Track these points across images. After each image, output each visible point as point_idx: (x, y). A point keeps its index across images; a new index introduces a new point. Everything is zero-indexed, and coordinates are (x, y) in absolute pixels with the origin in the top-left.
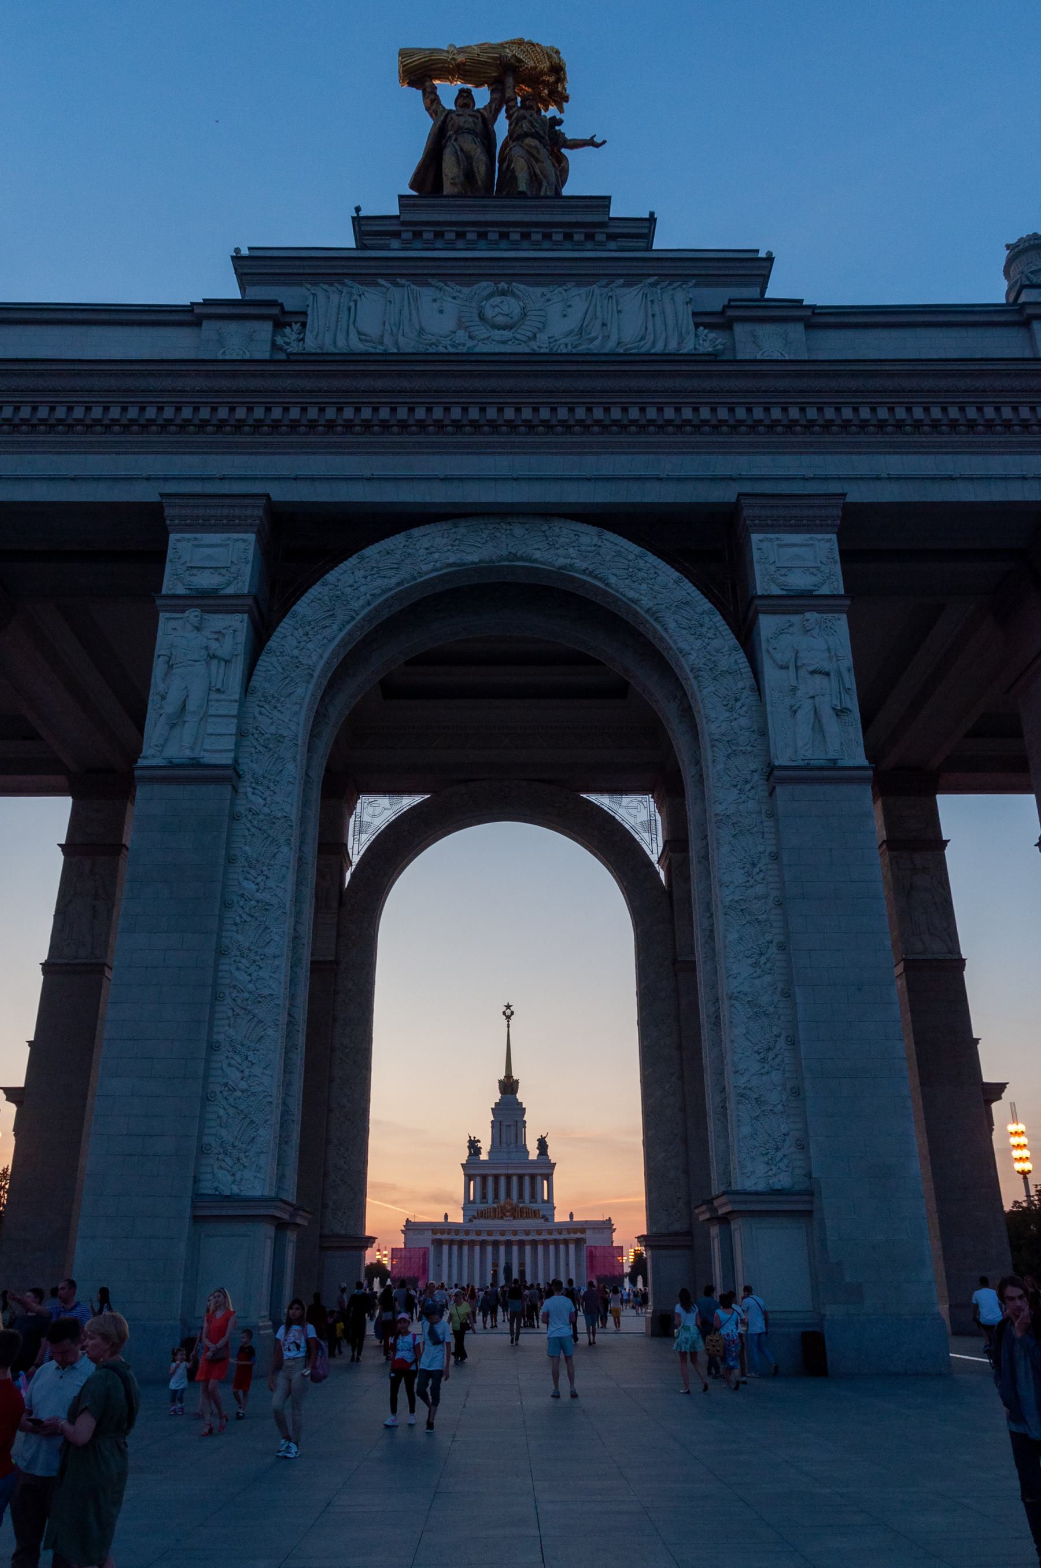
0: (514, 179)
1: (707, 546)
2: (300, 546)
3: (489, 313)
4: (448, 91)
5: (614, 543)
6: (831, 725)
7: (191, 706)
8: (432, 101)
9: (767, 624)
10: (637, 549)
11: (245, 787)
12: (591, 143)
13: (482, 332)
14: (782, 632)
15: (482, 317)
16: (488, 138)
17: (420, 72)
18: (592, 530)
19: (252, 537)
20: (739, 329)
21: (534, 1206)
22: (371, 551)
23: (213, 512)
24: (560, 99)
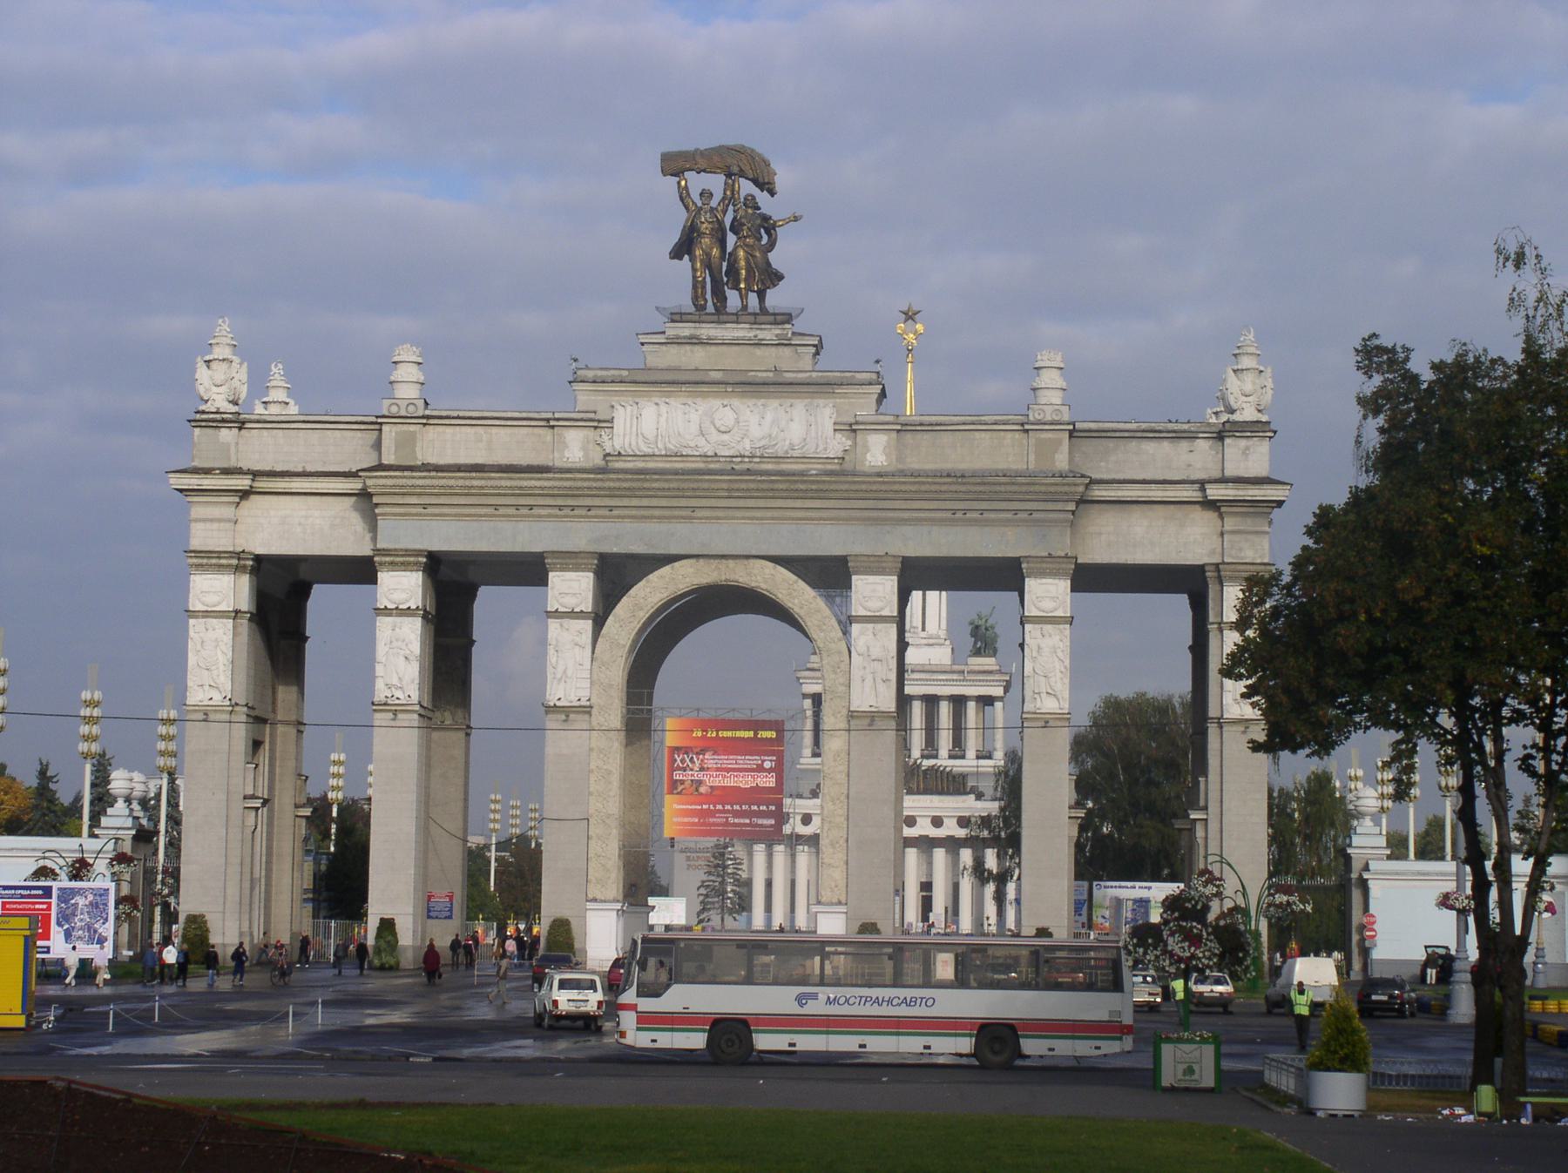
0: (737, 273)
1: (830, 575)
2: (616, 574)
3: (718, 424)
4: (696, 182)
5: (783, 572)
6: (881, 687)
7: (569, 673)
8: (684, 195)
9: (856, 628)
10: (795, 578)
11: (594, 711)
12: (796, 219)
13: (715, 436)
14: (862, 633)
15: (713, 423)
16: (721, 223)
17: (675, 165)
18: (771, 565)
19: (591, 575)
20: (860, 436)
21: (968, 764)
22: (654, 577)
23: (570, 559)
24: (772, 193)
